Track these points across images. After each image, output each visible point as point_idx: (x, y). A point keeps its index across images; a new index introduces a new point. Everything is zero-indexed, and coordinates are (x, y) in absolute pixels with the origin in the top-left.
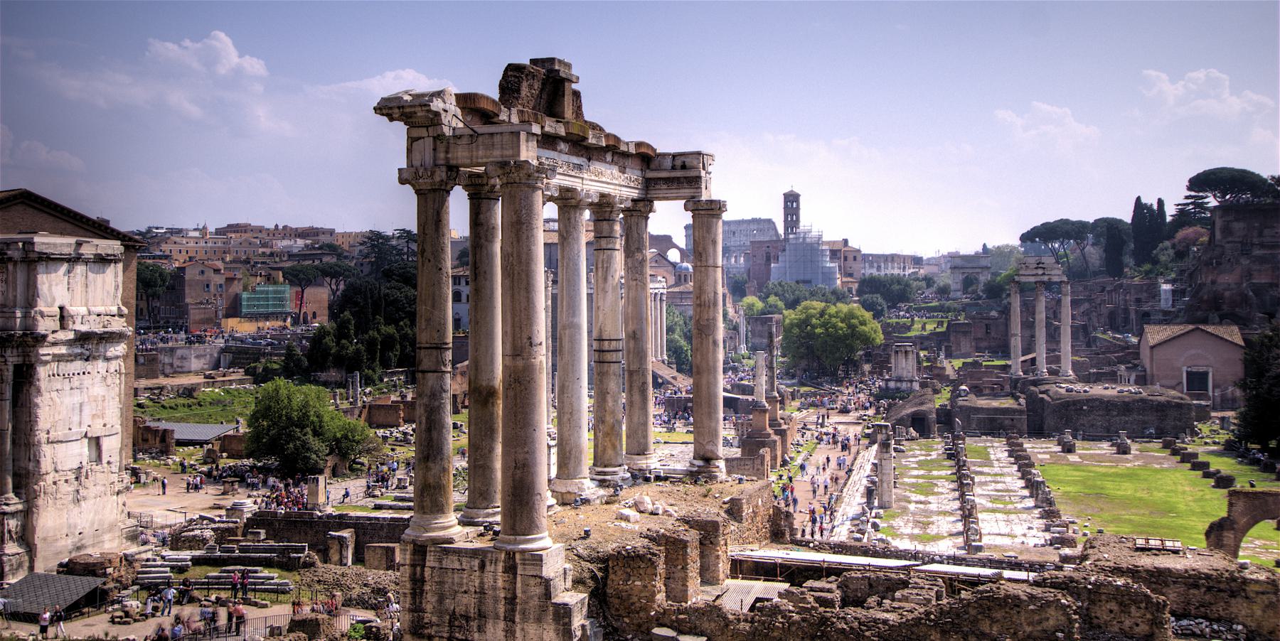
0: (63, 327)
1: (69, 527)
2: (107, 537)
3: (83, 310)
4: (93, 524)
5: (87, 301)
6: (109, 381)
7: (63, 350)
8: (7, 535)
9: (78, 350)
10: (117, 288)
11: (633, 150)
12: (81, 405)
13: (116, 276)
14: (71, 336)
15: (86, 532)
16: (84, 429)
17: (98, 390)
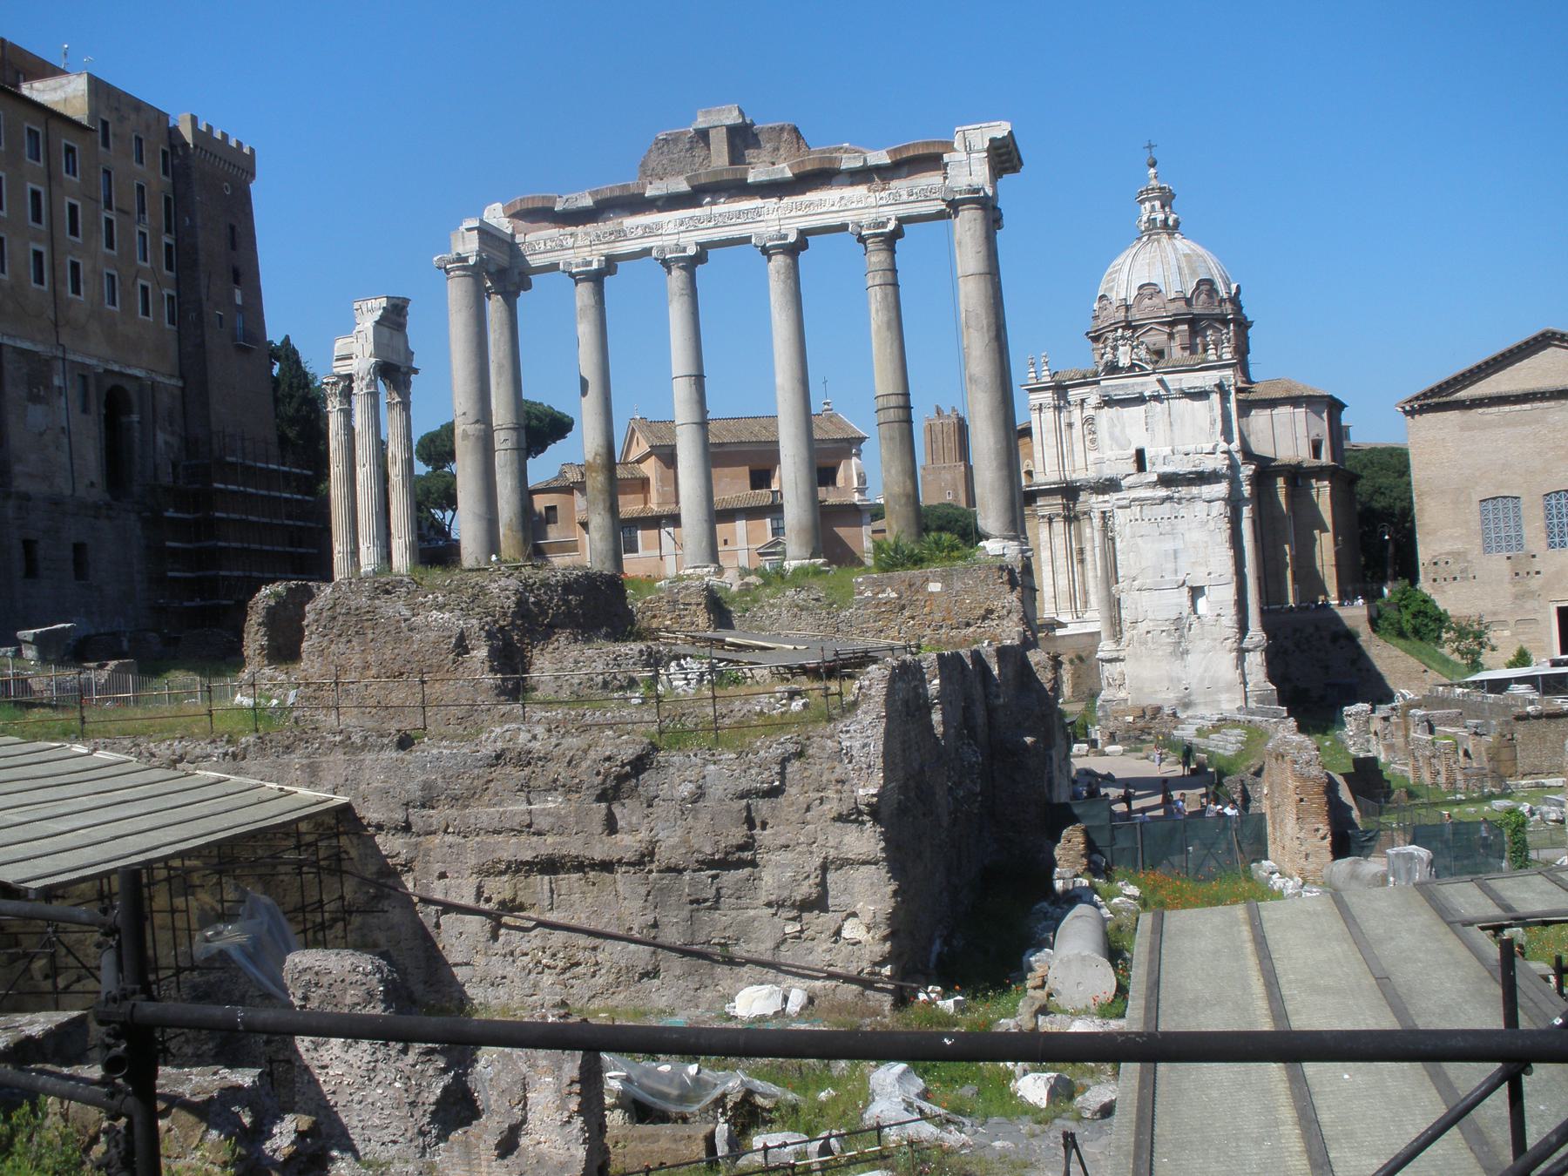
0: (1141, 466)
1: (1171, 680)
2: (1224, 697)
3: (1167, 450)
4: (1202, 679)
5: (1172, 439)
6: (1212, 525)
7: (1148, 493)
8: (1104, 683)
9: (1162, 492)
10: (1213, 423)
11: (881, 158)
12: (1175, 552)
13: (1211, 409)
14: (1154, 478)
15: (1193, 687)
16: (1181, 578)
17: (1196, 536)
